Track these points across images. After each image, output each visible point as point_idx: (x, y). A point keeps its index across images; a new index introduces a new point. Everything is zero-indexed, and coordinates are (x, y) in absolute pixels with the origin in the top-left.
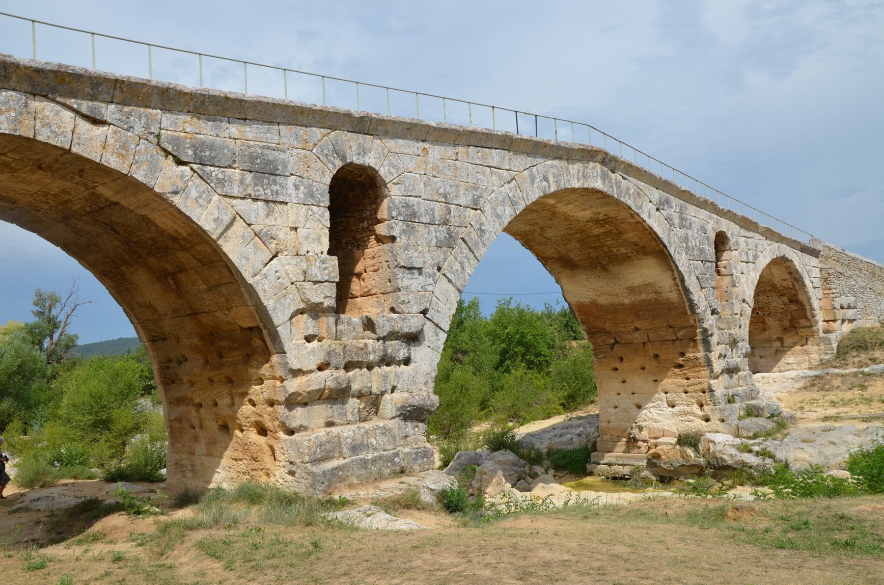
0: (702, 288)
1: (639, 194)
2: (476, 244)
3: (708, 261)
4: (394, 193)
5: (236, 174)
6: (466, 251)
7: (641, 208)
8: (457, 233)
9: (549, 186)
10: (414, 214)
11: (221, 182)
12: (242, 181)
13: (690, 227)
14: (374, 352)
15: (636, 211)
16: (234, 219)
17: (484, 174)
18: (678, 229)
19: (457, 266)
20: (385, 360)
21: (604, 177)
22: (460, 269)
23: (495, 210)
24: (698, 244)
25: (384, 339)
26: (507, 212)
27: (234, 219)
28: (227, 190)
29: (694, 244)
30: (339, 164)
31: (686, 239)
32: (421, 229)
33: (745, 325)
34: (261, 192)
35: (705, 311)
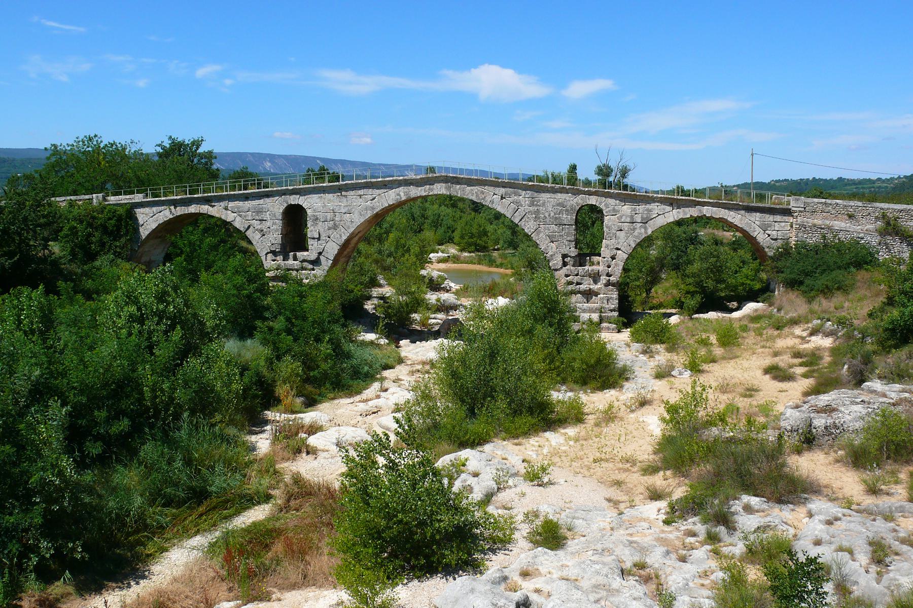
0: (552, 242)
1: (483, 193)
2: (349, 228)
3: (565, 225)
4: (309, 212)
5: (250, 213)
6: (343, 230)
7: (484, 199)
8: (339, 224)
9: (401, 198)
10: (317, 219)
11: (245, 216)
12: (252, 215)
13: (544, 204)
14: (297, 266)
15: (479, 201)
16: (249, 227)
17: (356, 198)
18: (526, 207)
19: (339, 236)
20: (303, 269)
21: (448, 188)
22: (339, 237)
23: (360, 213)
24: (552, 214)
25: (302, 262)
26: (368, 212)
27: (249, 227)
28: (247, 218)
29: (547, 215)
30: (286, 205)
31: (538, 212)
32: (320, 223)
33: (616, 265)
34: (257, 218)
35: (551, 256)
